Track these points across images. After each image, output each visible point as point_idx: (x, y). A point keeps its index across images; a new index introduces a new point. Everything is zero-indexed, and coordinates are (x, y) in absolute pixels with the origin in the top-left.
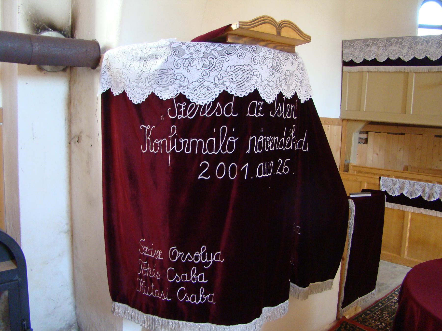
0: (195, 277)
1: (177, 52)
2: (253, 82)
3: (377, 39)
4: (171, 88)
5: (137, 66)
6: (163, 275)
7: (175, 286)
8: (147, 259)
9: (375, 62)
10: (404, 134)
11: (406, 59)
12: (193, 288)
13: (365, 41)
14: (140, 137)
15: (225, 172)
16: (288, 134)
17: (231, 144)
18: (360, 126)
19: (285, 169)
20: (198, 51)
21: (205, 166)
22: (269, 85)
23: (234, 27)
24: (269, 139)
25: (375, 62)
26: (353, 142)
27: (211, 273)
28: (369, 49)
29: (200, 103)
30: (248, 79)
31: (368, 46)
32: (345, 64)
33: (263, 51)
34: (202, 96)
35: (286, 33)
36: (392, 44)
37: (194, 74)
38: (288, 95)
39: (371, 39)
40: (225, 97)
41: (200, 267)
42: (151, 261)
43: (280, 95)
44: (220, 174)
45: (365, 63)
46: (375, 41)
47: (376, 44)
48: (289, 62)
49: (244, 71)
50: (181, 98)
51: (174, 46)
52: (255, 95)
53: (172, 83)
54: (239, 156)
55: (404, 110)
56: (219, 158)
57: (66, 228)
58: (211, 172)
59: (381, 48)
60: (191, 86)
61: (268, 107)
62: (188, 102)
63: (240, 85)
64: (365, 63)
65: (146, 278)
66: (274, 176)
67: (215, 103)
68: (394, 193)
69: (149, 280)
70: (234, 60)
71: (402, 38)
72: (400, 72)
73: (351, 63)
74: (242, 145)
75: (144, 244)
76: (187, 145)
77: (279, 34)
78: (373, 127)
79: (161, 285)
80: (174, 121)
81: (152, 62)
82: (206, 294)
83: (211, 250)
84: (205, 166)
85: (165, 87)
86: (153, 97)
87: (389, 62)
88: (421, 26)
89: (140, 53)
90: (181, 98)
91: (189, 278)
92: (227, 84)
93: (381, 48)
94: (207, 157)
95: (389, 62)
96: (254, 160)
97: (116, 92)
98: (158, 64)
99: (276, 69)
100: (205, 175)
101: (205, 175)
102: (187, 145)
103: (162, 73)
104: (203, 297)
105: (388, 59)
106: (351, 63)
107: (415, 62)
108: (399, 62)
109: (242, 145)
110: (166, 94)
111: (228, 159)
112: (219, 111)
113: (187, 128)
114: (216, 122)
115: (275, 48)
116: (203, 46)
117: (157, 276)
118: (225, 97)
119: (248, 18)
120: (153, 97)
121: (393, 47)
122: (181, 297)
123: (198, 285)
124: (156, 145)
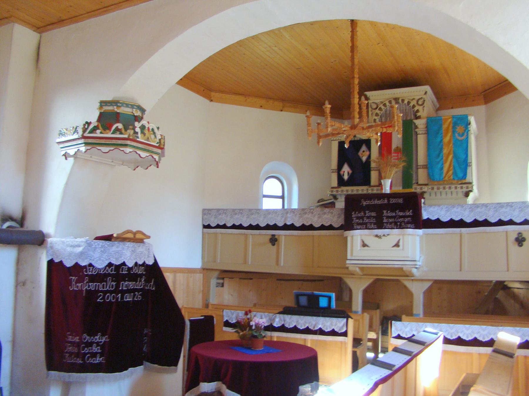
0: (96, 349)
1: (89, 245)
2: (123, 258)
3: (226, 210)
4: (86, 260)
5: (69, 249)
6: (79, 349)
7: (85, 354)
8: (70, 342)
9: (224, 227)
10: (252, 279)
11: (245, 225)
12: (94, 355)
13: (218, 210)
14: (70, 283)
15: (110, 298)
16: (140, 281)
17: (113, 285)
18: (216, 274)
19: (138, 297)
20: (99, 245)
21: (101, 295)
22: (130, 259)
23: (115, 235)
24: (130, 283)
25: (224, 227)
26: (212, 286)
27: (103, 347)
28: (220, 216)
29: (99, 267)
30: (121, 257)
31: (220, 214)
32: (205, 227)
33: (128, 244)
34: (100, 264)
35: (138, 236)
36: (236, 214)
37: (97, 255)
38: (140, 262)
39: (222, 209)
40: (110, 265)
41: (98, 344)
42: (73, 343)
43: (136, 263)
44: (108, 299)
45: (218, 226)
46: (224, 211)
47: (226, 213)
48: (140, 248)
49: (119, 253)
50: (91, 265)
51: (88, 242)
52: (124, 264)
53: (87, 258)
54: (116, 291)
55: (245, 262)
56: (108, 292)
57: (10, 339)
58: (103, 298)
59: (229, 216)
60: (95, 260)
61: (130, 269)
62: (94, 267)
63: (117, 259)
64: (218, 226)
65: (69, 353)
66: (133, 301)
67: (106, 267)
68: (232, 321)
69: (71, 354)
70: (114, 249)
71: (242, 210)
72: (242, 234)
73: (208, 227)
74: (118, 286)
75: (70, 335)
76: (92, 286)
77: (135, 237)
78: (226, 275)
79: (77, 355)
80: (87, 275)
81: (77, 248)
82: (100, 358)
83: (103, 335)
84: (101, 295)
85: (83, 260)
86: (77, 264)
87: (234, 227)
88: (265, 196)
89: (71, 243)
90: (91, 265)
91: (92, 349)
92: (112, 259)
93: (229, 216)
94: (101, 291)
95: (234, 227)
96: (123, 292)
97: (57, 261)
98: (80, 249)
99: (133, 251)
100: (101, 299)
101: (101, 299)
102: (92, 286)
103: (82, 253)
104: (98, 360)
105: (234, 225)
106: (208, 227)
107: (251, 227)
108: (240, 227)
109: (118, 286)
110: (83, 263)
111: (111, 292)
112: (107, 271)
113: (94, 278)
114: (106, 275)
115: (134, 242)
116: (101, 242)
117: (76, 350)
118: (110, 265)
119: (120, 232)
120: (77, 264)
121: (236, 216)
122: (88, 360)
123: (97, 353)
124: (78, 286)
